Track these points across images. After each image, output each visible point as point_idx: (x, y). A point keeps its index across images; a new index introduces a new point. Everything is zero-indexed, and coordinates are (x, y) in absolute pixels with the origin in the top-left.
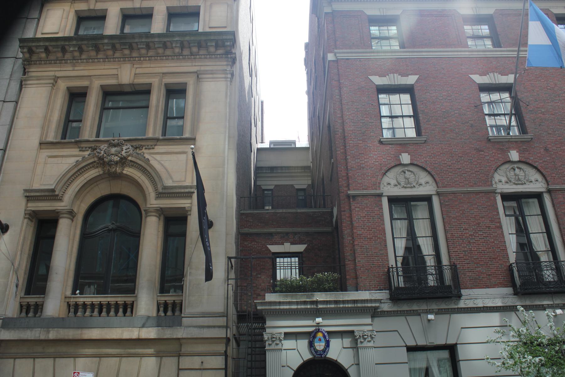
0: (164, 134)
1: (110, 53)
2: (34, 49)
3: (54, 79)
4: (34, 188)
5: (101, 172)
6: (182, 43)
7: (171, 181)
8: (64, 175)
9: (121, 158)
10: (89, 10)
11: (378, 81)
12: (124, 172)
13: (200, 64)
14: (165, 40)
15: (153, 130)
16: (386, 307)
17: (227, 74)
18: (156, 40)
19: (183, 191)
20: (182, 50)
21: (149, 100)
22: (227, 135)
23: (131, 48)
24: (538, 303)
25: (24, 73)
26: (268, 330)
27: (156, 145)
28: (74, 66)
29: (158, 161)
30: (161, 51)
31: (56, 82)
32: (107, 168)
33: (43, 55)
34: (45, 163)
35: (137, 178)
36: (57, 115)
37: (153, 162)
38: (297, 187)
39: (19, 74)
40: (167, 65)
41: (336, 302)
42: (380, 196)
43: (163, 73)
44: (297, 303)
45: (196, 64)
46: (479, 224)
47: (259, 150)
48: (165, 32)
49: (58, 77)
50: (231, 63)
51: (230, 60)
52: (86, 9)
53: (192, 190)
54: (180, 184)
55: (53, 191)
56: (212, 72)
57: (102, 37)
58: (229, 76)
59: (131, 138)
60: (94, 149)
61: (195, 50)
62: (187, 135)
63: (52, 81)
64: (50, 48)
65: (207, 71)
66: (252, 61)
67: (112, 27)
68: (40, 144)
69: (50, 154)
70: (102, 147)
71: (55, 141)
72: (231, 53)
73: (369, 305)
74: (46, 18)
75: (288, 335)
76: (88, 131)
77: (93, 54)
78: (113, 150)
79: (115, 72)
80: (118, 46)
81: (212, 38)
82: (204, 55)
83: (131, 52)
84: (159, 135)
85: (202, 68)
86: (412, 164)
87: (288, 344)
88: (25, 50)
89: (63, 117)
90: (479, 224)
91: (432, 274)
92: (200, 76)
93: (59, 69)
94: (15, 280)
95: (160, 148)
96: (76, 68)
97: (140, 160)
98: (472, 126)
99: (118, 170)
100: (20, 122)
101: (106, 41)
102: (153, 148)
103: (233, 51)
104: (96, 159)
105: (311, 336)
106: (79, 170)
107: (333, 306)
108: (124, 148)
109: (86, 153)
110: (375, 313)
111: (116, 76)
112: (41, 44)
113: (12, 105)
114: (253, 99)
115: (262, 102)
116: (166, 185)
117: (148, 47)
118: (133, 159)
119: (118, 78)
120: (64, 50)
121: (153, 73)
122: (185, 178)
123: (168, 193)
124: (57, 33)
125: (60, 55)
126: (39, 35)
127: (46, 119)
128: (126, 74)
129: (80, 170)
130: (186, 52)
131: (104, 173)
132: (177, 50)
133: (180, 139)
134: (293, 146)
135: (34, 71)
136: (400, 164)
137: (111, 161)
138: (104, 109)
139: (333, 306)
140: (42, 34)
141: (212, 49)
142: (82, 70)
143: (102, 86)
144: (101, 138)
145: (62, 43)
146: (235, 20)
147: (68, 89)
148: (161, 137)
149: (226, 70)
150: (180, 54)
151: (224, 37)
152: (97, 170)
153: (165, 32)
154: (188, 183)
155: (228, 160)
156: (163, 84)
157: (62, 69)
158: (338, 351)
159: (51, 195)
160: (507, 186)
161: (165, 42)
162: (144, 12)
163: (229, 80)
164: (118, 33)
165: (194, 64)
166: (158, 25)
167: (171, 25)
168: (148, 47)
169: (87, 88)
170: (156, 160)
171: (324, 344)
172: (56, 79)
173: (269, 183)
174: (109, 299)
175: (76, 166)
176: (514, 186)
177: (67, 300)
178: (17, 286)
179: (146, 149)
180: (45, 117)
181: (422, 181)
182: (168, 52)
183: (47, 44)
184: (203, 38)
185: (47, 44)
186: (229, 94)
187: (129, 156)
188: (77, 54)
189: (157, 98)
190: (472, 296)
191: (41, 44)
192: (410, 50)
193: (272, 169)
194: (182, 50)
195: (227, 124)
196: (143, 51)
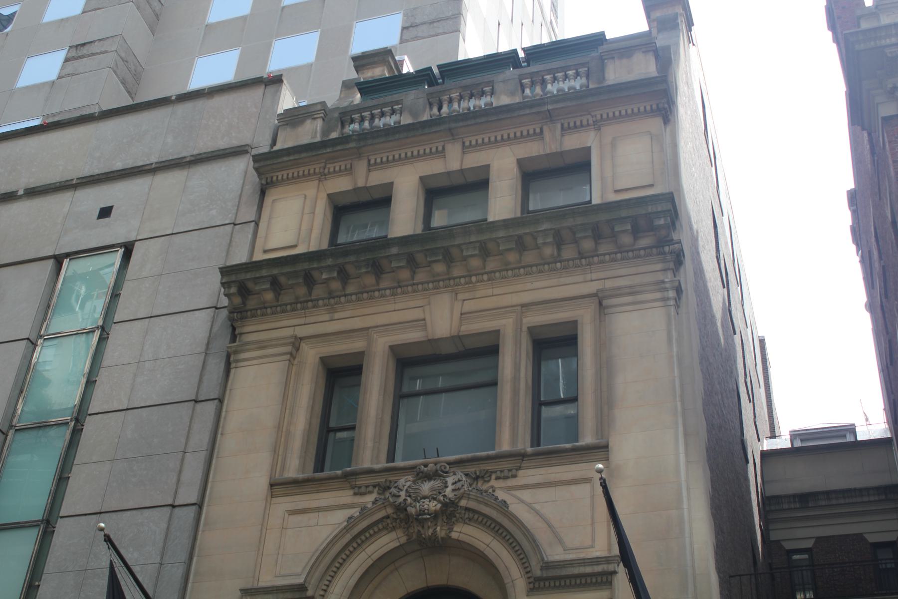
0: (536, 440)
1: (405, 274)
2: (250, 285)
3: (293, 344)
4: (262, 584)
5: (404, 540)
6: (557, 234)
7: (560, 549)
8: (324, 553)
9: (445, 505)
10: (356, 190)
12: (454, 535)
13: (601, 275)
14: (520, 232)
15: (511, 435)
17: (666, 289)
18: (501, 234)
19: (588, 570)
20: (559, 250)
21: (496, 367)
22: (681, 429)
23: (449, 259)
25: (234, 338)
27: (520, 468)
28: (332, 310)
29: (529, 506)
30: (512, 257)
31: (298, 349)
32: (416, 528)
33: (269, 296)
34: (284, 528)
35: (482, 547)
36: (302, 422)
37: (516, 508)
38: (872, 539)
39: (223, 342)
40: (529, 286)
43: (523, 306)
45: (594, 276)
47: (766, 455)
48: (519, 215)
49: (301, 339)
50: (672, 265)
51: (669, 257)
52: (350, 188)
53: (611, 567)
54: (582, 556)
55: (302, 588)
56: (632, 291)
57: (385, 242)
58: (672, 294)
59: (464, 456)
60: (384, 488)
61: (587, 245)
62: (588, 439)
63: (289, 349)
64: (283, 280)
65: (619, 288)
66: (725, 250)
67: (404, 219)
68: (272, 485)
69: (292, 506)
70: (402, 482)
71: (301, 476)
72: (671, 242)
74: (270, 218)
76: (369, 453)
77: (370, 280)
78: (426, 487)
79: (417, 314)
80: (420, 257)
81: (624, 213)
82: (609, 254)
83: (449, 267)
84: (524, 444)
85: (609, 284)
88: (233, 290)
89: (317, 422)
92: (605, 302)
93: (302, 321)
95: (529, 475)
96: (337, 316)
97: (486, 505)
99: (441, 532)
100: (229, 443)
101: (394, 250)
102: (515, 476)
103: (675, 237)
104: (390, 511)
106: (354, 539)
108: (450, 480)
109: (369, 499)
111: (421, 323)
112: (264, 272)
113: (211, 407)
114: (737, 338)
115: (762, 342)
116: (551, 559)
117: (485, 252)
118: (472, 504)
119: (425, 325)
120: (309, 281)
121: (503, 305)
122: (593, 540)
123: (555, 578)
124: (294, 246)
125: (302, 291)
126: (259, 256)
127: (282, 431)
128: (441, 316)
129: (355, 539)
130: (568, 252)
131: (409, 541)
132: (548, 251)
133: (574, 450)
134: (850, 438)
135: (253, 331)
137: (422, 512)
138: (401, 396)
140: (265, 252)
141: (626, 239)
142: (349, 318)
143: (393, 349)
144: (399, 463)
145: (306, 266)
146: (672, 167)
147: (324, 360)
148: (529, 450)
149: (663, 282)
150: (557, 259)
151: (650, 209)
152: (393, 535)
153: (519, 215)
154: (599, 550)
155: (688, 489)
156: (525, 329)
157: (308, 320)
161: (520, 237)
162: (471, 178)
163: (672, 302)
164: (419, 231)
165: (588, 277)
166: (502, 203)
167: (531, 196)
168: (485, 252)
169: (361, 354)
170: (523, 502)
172: (296, 343)
173: (801, 535)
175: (347, 529)
179: (497, 478)
180: (279, 427)
182: (530, 257)
183: (275, 271)
184: (603, 217)
185: (275, 271)
186: (674, 334)
187: (461, 498)
188: (336, 285)
189: (514, 364)
191: (264, 272)
193: (804, 499)
194: (559, 250)
195: (679, 404)
196: (475, 263)
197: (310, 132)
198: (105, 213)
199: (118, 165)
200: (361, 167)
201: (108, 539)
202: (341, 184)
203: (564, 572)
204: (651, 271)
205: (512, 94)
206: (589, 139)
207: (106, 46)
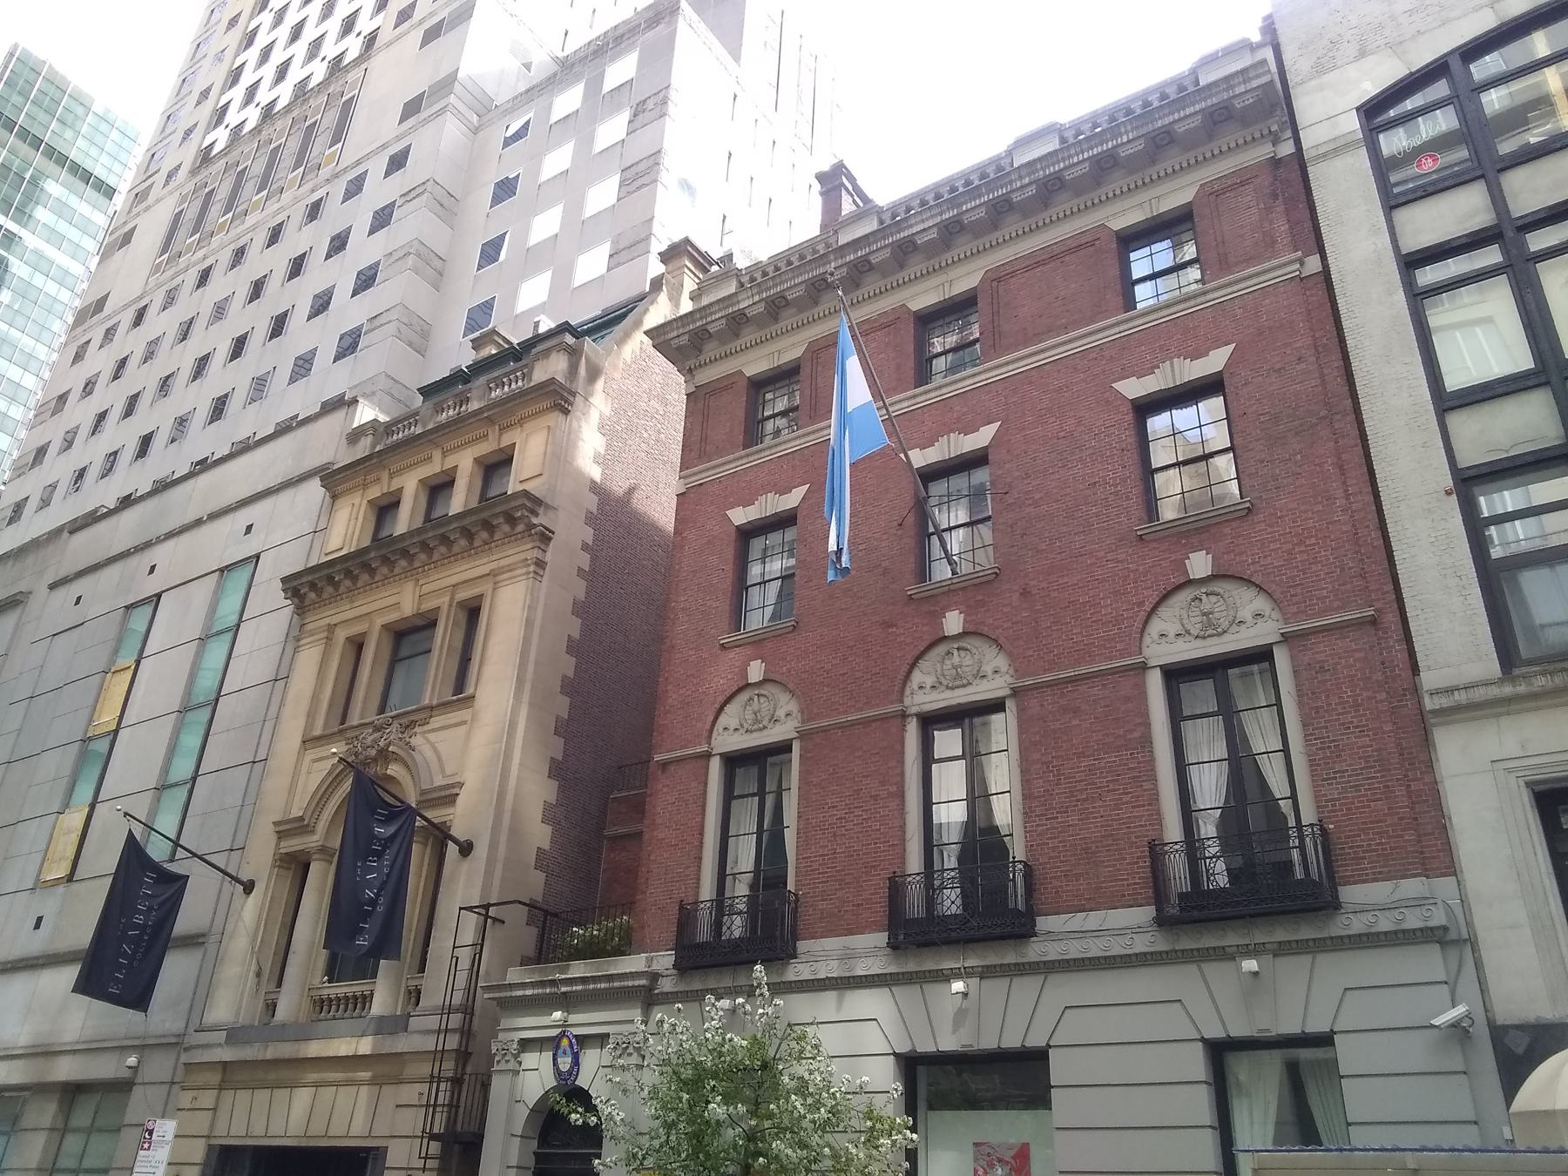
11: (740, 516)
16: (666, 985)
18: (430, 534)
19: (443, 793)
24: (930, 965)
26: (501, 1036)
39: (295, 633)
41: (584, 980)
42: (708, 756)
44: (533, 985)
46: (858, 791)
55: (301, 819)
56: (510, 568)
69: (313, 757)
73: (630, 983)
75: (526, 1045)
81: (498, 510)
85: (503, 562)
86: (765, 681)
87: (530, 1059)
90: (858, 791)
91: (740, 913)
94: (254, 967)
95: (437, 721)
98: (886, 571)
100: (288, 710)
101: (372, 555)
105: (553, 1044)
107: (580, 988)
110: (648, 996)
112: (304, 580)
127: (315, 697)
128: (402, 599)
136: (748, 685)
138: (395, 661)
139: (580, 988)
143: (385, 627)
145: (325, 572)
158: (592, 1071)
159: (299, 827)
160: (935, 696)
171: (570, 1060)
172: (331, 628)
174: (354, 989)
175: (329, 773)
176: (948, 694)
177: (314, 993)
178: (258, 975)
181: (781, 713)
190: (820, 955)
191: (304, 580)
192: (810, 429)
197: (364, 448)
198: (249, 529)
199: (260, 488)
200: (437, 455)
201: (126, 814)
202: (375, 492)
203: (435, 795)
204: (526, 550)
205: (480, 399)
206: (513, 436)
207: (393, 315)
